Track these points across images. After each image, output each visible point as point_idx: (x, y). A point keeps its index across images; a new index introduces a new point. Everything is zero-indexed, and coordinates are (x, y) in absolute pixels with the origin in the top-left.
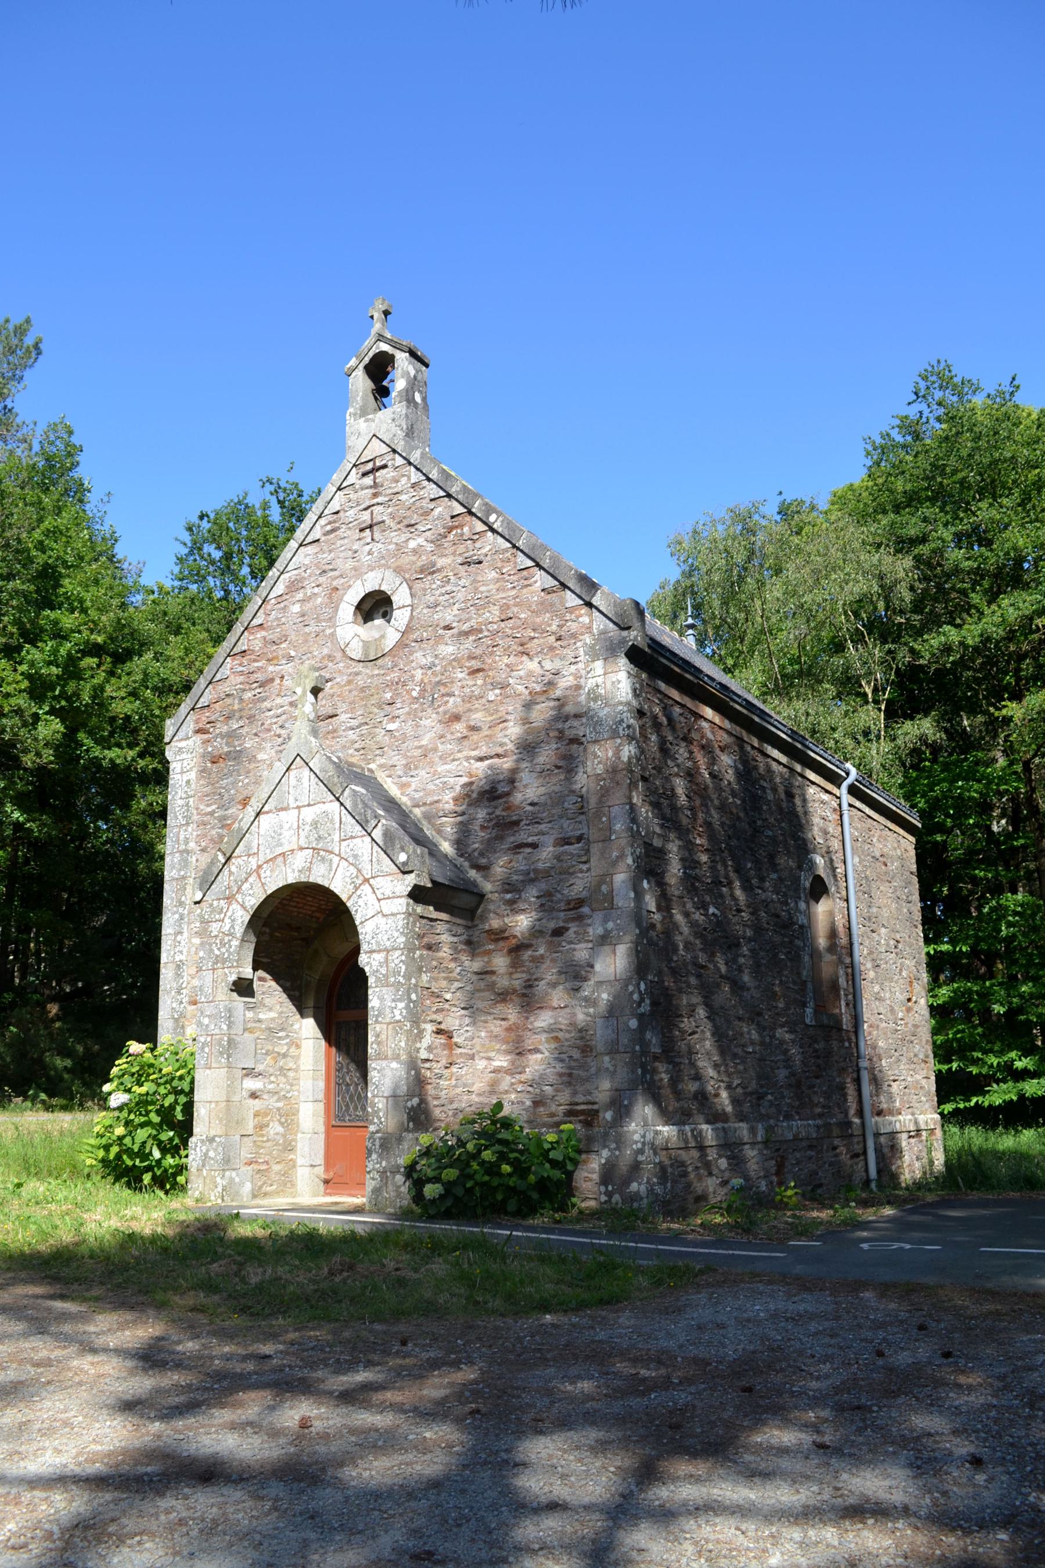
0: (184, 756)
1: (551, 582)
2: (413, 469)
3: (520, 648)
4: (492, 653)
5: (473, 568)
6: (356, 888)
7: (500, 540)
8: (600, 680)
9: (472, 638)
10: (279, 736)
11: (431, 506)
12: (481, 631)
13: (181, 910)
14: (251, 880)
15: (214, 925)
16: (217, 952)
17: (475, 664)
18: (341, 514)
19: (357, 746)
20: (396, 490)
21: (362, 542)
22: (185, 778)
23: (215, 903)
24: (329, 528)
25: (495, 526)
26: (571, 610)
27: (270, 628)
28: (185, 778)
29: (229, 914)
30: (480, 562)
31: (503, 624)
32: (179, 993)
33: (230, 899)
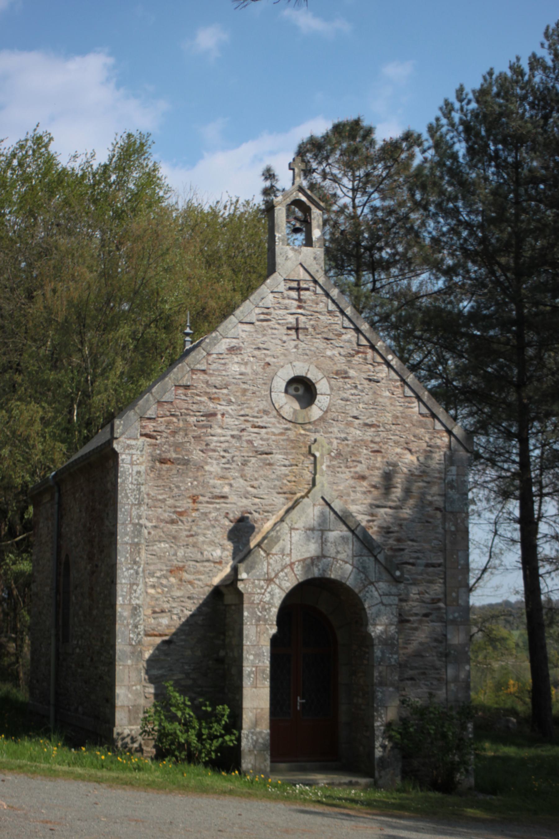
0: (134, 451)
1: (425, 411)
2: (330, 301)
3: (406, 446)
4: (386, 443)
5: (373, 384)
6: (365, 587)
7: (393, 373)
8: (454, 477)
9: (373, 429)
10: (223, 457)
11: (343, 331)
12: (379, 426)
13: (135, 567)
14: (286, 570)
15: (256, 596)
16: (259, 614)
17: (376, 447)
18: (272, 310)
19: (289, 478)
20: (316, 310)
21: (290, 337)
22: (136, 468)
23: (256, 582)
24: (262, 317)
25: (392, 363)
26: (438, 432)
27: (211, 375)
28: (136, 468)
29: (269, 590)
30: (378, 382)
31: (394, 427)
32: (136, 627)
33: (269, 581)
